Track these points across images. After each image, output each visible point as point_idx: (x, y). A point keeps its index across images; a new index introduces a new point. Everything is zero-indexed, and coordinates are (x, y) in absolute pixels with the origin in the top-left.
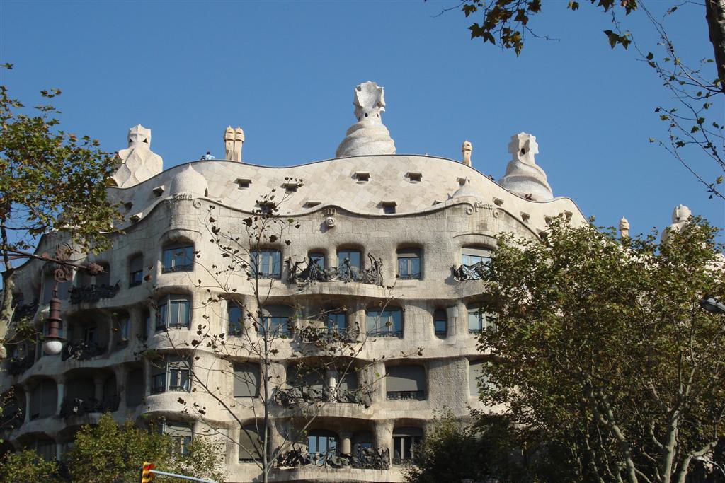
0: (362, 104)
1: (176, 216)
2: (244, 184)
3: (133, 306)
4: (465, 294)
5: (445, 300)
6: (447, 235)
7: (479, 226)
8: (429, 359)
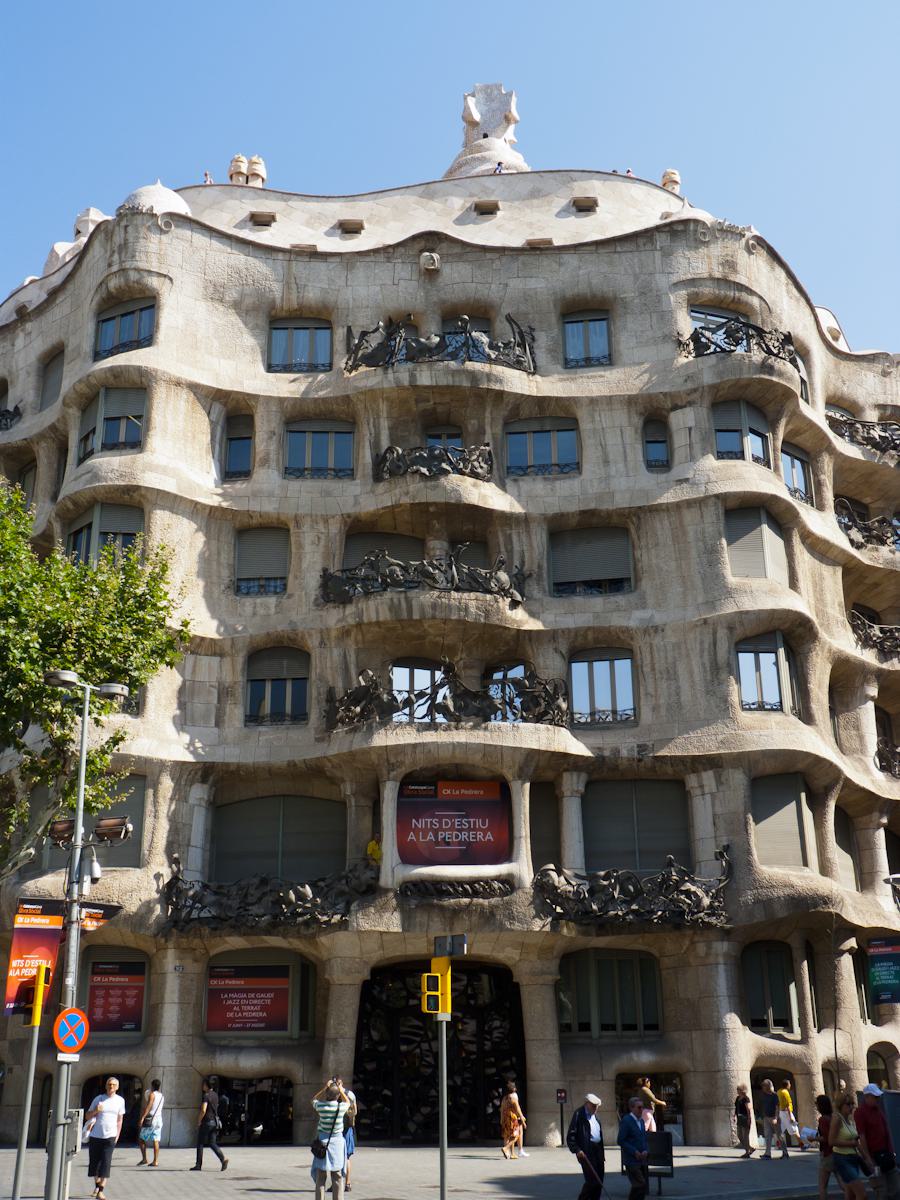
0: (477, 117)
1: (124, 247)
2: (261, 221)
3: (41, 436)
4: (708, 378)
5: (665, 394)
6: (662, 281)
7: (722, 264)
8: (640, 508)
